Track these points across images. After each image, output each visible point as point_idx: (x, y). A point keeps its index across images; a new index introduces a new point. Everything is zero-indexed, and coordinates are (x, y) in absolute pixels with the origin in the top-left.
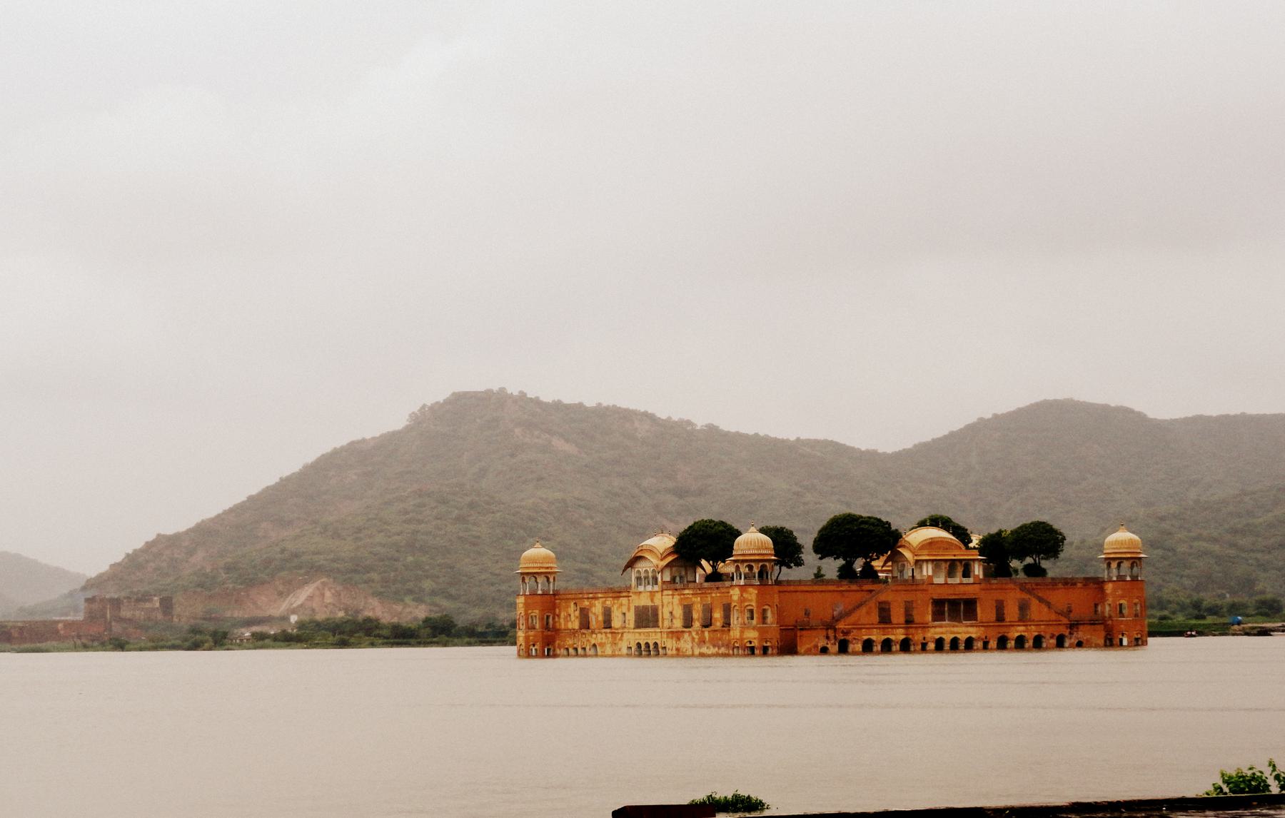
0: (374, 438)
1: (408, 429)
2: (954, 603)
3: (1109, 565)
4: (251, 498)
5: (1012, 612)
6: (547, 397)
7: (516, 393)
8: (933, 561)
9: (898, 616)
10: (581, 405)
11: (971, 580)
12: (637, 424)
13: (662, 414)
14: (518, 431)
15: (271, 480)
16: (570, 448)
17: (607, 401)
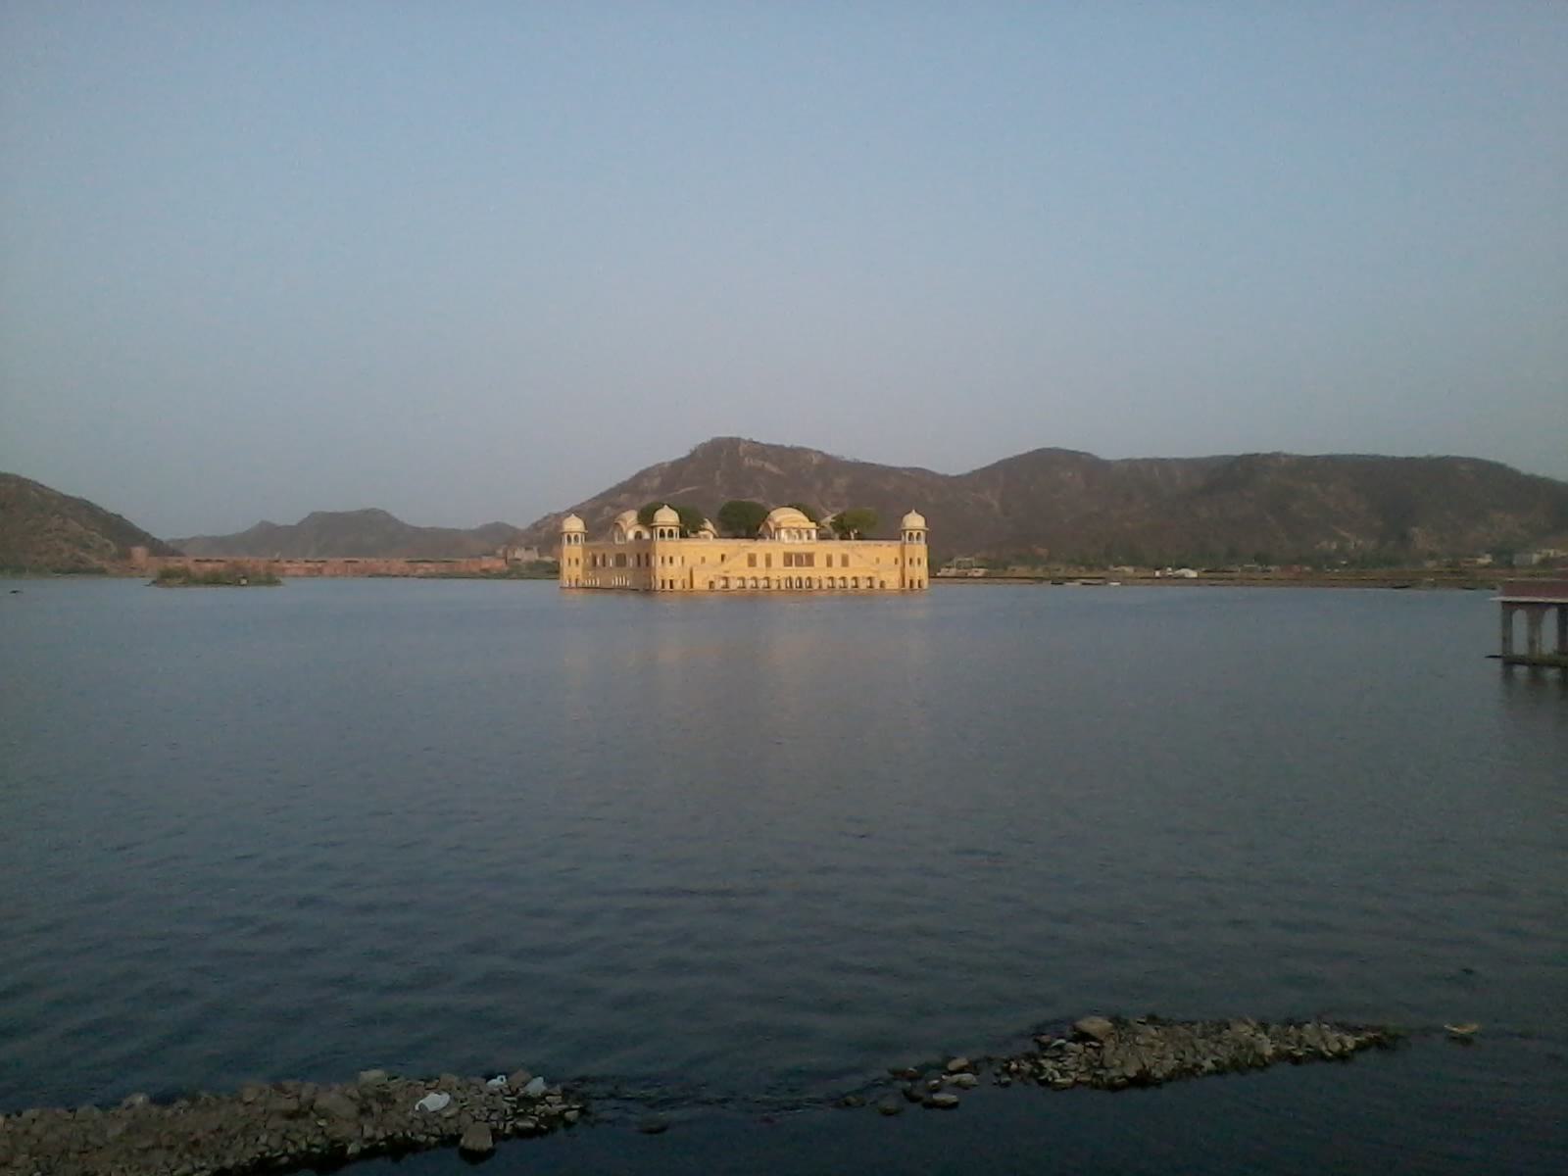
2: (799, 556)
3: (905, 534)
5: (837, 562)
6: (764, 441)
7: (747, 438)
9: (761, 562)
10: (782, 447)
11: (810, 541)
12: (813, 457)
13: (828, 451)
14: (746, 459)
15: (613, 485)
16: (775, 470)
17: (797, 444)
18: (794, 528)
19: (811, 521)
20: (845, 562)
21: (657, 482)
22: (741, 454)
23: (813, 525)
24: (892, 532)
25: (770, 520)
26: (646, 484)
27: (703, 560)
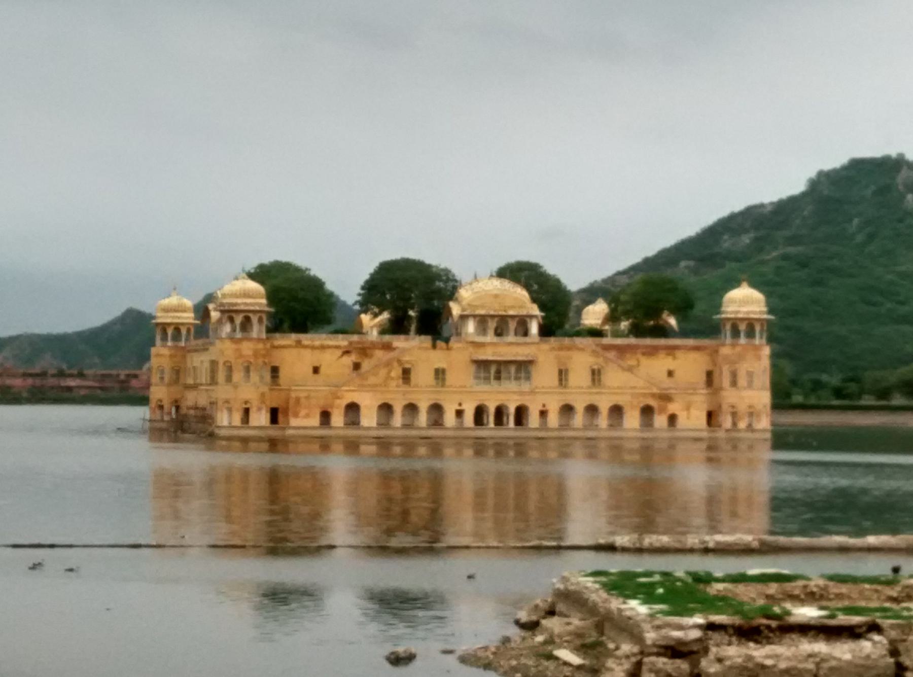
0: (772, 203)
1: (804, 195)
4: (647, 261)
5: (579, 377)
8: (474, 316)
11: (527, 339)
18: (493, 316)
19: (534, 300)
20: (596, 375)
21: (746, 239)
22: (901, 187)
23: (535, 310)
24: (705, 326)
25: (456, 300)
26: (727, 243)
27: (316, 370)
